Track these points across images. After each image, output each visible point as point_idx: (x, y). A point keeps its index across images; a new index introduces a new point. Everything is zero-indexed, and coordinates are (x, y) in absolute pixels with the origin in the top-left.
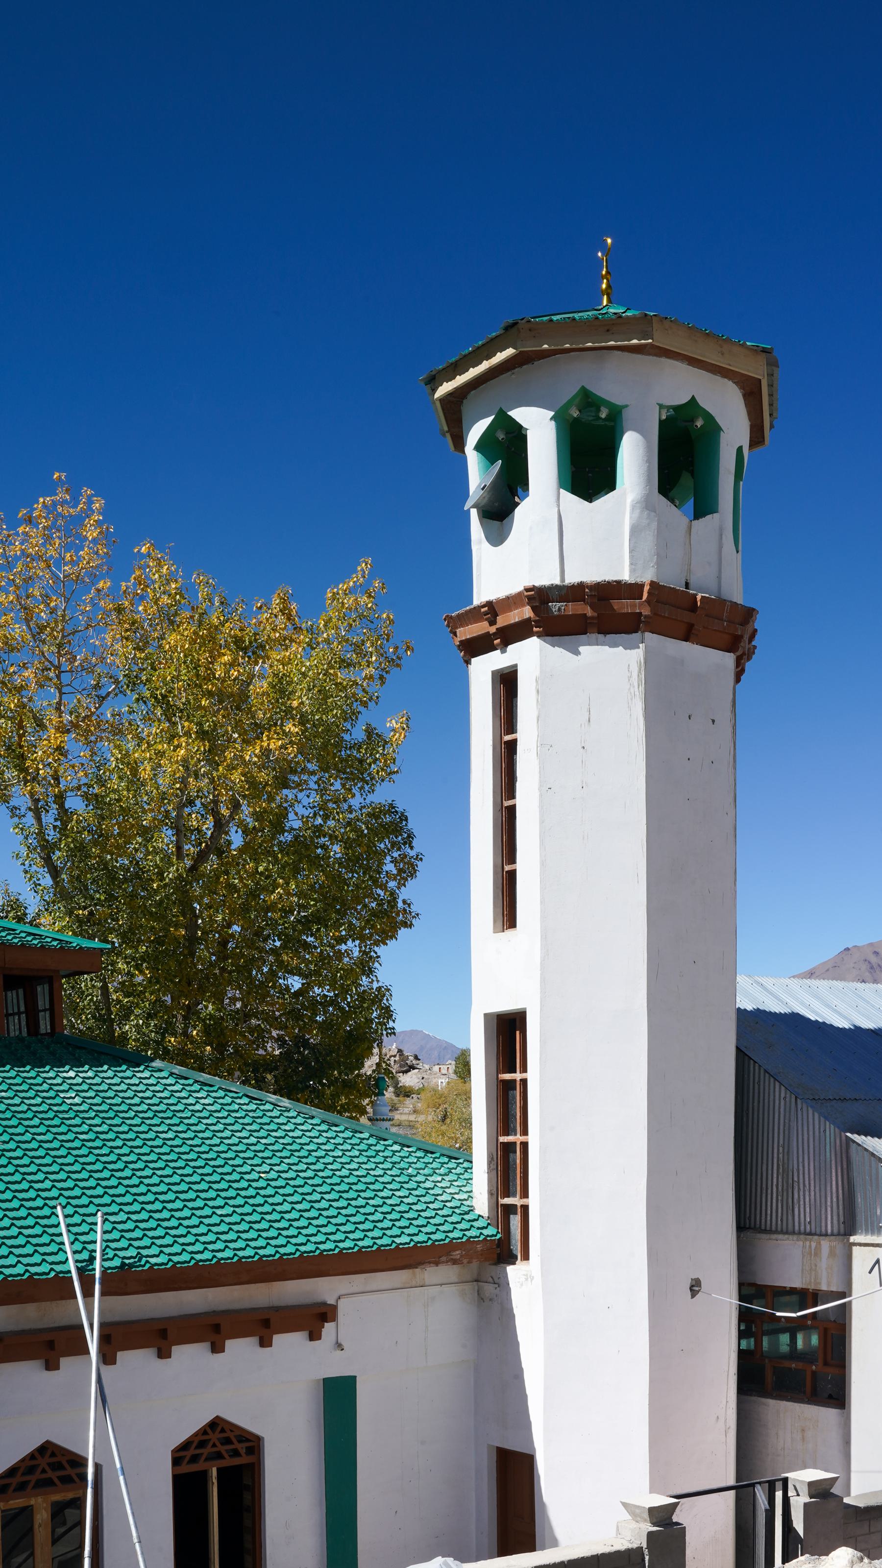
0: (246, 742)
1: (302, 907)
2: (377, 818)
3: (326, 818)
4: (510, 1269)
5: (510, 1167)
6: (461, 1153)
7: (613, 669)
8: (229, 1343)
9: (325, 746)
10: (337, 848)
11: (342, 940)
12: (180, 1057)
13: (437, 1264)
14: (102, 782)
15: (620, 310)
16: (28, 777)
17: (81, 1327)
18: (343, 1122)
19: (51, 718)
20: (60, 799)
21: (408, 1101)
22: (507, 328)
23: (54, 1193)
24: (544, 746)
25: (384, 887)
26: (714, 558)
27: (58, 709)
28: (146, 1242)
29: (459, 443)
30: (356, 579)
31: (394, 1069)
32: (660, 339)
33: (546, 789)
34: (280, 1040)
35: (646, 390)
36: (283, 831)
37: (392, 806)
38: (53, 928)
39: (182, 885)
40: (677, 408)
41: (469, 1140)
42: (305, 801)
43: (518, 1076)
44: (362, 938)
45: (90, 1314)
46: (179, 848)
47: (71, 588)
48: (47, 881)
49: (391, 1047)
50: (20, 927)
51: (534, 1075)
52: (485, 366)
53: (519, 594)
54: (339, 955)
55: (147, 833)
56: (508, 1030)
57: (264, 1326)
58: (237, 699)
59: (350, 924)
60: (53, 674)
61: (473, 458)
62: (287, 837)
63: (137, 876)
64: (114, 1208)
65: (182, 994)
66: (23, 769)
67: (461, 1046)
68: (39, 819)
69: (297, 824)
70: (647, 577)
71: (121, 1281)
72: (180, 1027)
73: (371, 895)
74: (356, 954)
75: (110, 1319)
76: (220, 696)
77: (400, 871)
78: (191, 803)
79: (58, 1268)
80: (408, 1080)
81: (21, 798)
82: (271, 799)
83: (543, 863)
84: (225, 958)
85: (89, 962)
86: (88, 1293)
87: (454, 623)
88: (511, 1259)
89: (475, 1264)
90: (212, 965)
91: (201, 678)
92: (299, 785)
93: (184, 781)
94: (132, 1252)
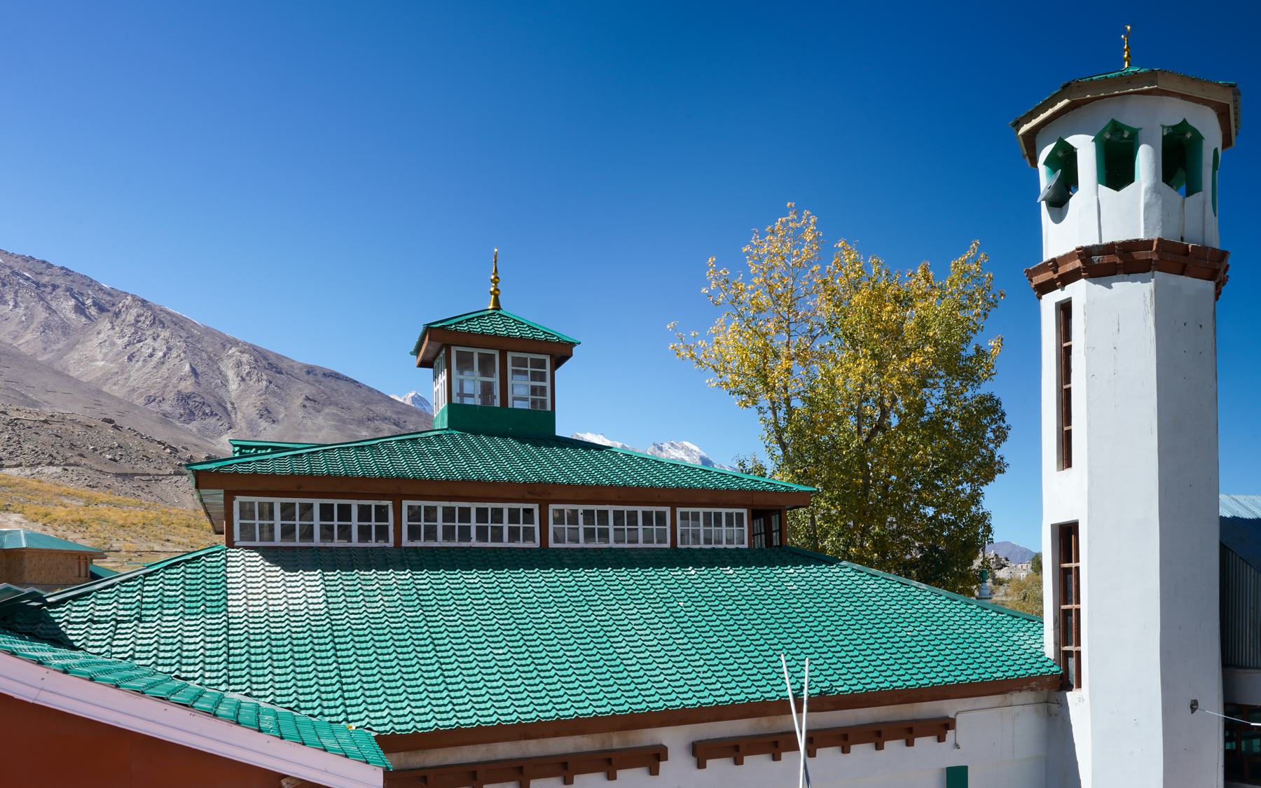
0: (901, 359)
1: (934, 463)
2: (982, 403)
3: (950, 404)
4: (1068, 694)
5: (1068, 627)
6: (1038, 618)
7: (1133, 298)
8: (887, 744)
9: (949, 359)
10: (957, 424)
11: (960, 483)
12: (859, 559)
13: (1020, 691)
14: (812, 389)
15: (1136, 69)
16: (769, 388)
17: (795, 733)
18: (961, 598)
19: (784, 350)
20: (788, 400)
21: (1001, 588)
22: (1064, 87)
23: (780, 646)
24: (1089, 348)
25: (986, 447)
26: (1200, 221)
27: (787, 346)
28: (836, 677)
29: (1034, 161)
30: (970, 253)
31: (993, 566)
32: (1162, 84)
33: (1091, 376)
34: (921, 549)
35: (1153, 117)
36: (923, 415)
37: (992, 396)
38: (782, 480)
39: (861, 450)
40: (1174, 127)
41: (1042, 611)
42: (937, 395)
43: (1073, 565)
44: (973, 481)
45: (800, 724)
46: (859, 428)
47: (796, 271)
48: (779, 452)
49: (990, 553)
50: (761, 479)
51: (1083, 564)
52: (1050, 111)
53: (1073, 252)
54: (958, 493)
55: (839, 420)
56: (1066, 535)
57: (909, 732)
58: (896, 333)
59: (965, 473)
60: (786, 325)
61: (1042, 169)
62: (926, 418)
63: (833, 447)
64: (816, 656)
65: (860, 520)
66: (766, 384)
67: (1036, 551)
68: (775, 414)
69: (932, 410)
70: (1155, 235)
71: (820, 702)
72: (858, 542)
73: (978, 454)
74: (968, 491)
75: (812, 727)
76: (884, 332)
77: (997, 437)
78: (867, 400)
79: (781, 694)
80: (1002, 574)
81: (764, 401)
82: (916, 394)
83: (1089, 425)
84: (886, 497)
85: (802, 500)
86: (799, 711)
87: (1031, 274)
88: (1070, 688)
89: (1045, 691)
90: (879, 501)
91: (873, 320)
92: (933, 385)
93: (862, 386)
94: (827, 684)
